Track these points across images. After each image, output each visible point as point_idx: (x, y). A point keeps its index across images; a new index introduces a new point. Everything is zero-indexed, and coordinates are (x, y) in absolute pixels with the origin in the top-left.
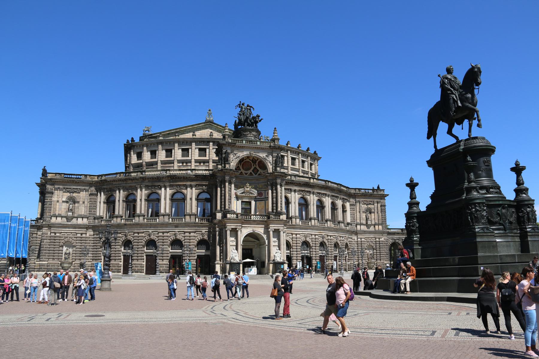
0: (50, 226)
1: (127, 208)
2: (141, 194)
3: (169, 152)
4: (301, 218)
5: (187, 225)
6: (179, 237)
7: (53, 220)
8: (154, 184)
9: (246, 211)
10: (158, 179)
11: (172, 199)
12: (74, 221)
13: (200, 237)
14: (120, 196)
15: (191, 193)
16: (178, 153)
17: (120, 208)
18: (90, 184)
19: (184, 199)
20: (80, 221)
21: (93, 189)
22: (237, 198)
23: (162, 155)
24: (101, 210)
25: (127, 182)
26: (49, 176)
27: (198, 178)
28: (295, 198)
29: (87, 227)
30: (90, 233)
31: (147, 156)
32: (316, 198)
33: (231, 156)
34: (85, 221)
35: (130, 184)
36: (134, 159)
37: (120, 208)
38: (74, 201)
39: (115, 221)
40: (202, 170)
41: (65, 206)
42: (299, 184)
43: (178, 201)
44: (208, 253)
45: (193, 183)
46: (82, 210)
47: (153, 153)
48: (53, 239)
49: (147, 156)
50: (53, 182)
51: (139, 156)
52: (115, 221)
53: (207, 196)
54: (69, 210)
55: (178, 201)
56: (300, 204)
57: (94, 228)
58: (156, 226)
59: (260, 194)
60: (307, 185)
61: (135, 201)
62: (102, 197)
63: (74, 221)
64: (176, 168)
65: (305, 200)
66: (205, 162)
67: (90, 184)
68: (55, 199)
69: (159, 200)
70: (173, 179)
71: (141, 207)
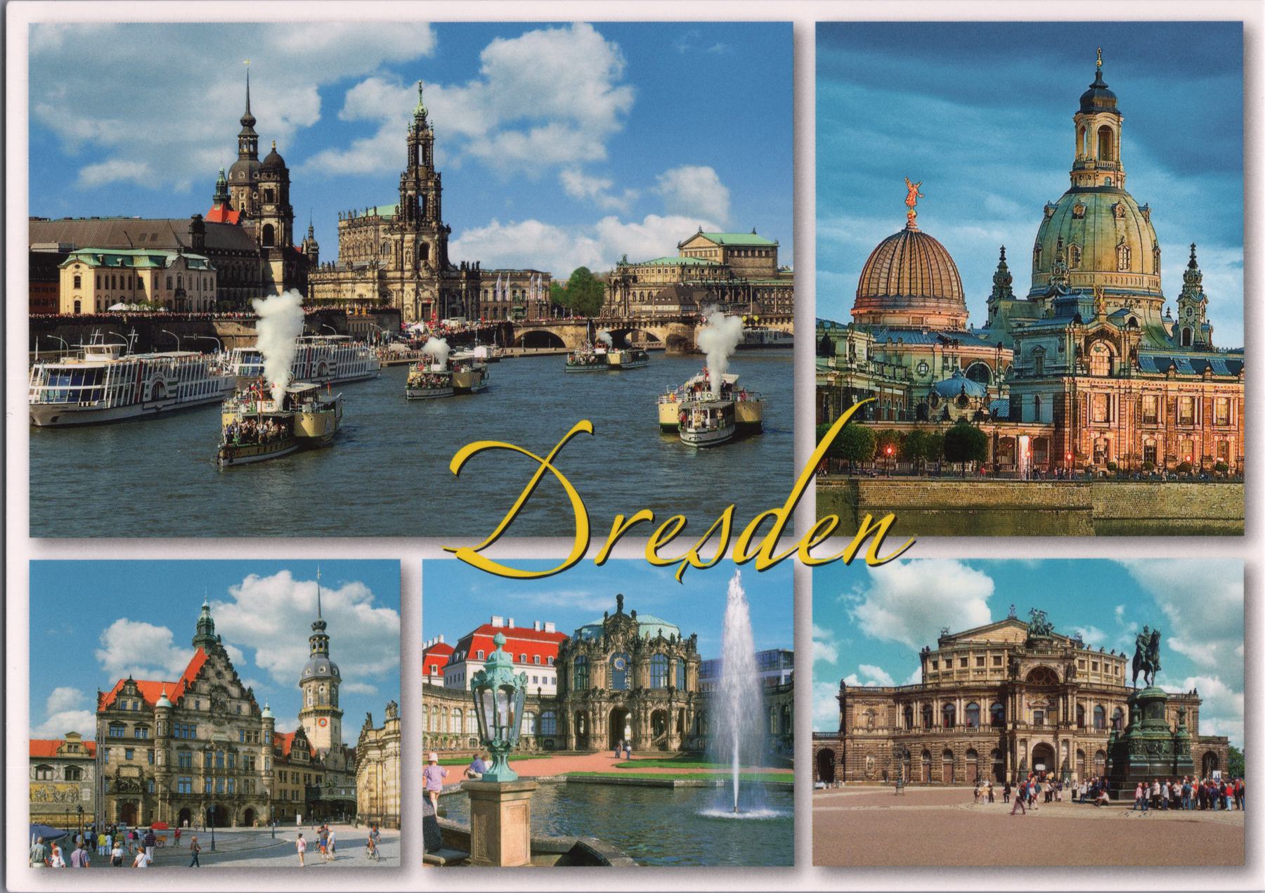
0: (852, 738)
1: (925, 718)
2: (937, 706)
3: (964, 662)
4: (1097, 727)
5: (980, 735)
6: (975, 747)
7: (855, 732)
8: (949, 695)
9: (1038, 721)
10: (953, 690)
11: (968, 711)
12: (875, 733)
13: (993, 747)
14: (917, 707)
15: (985, 705)
16: (973, 662)
17: (918, 719)
18: (888, 696)
19: (978, 710)
20: (880, 732)
21: (891, 701)
22: (1030, 707)
23: (957, 664)
24: (900, 721)
25: (922, 694)
26: (848, 690)
27: (991, 689)
28: (1090, 706)
29: (888, 738)
30: (891, 743)
31: (943, 666)
32: (1114, 706)
33: (1022, 668)
34: (886, 732)
35: (926, 696)
36: (931, 670)
37: (918, 719)
38: (874, 713)
39: (913, 732)
40: (996, 679)
41: (865, 719)
42: (1094, 693)
43: (973, 712)
44: (1001, 762)
45: (987, 694)
46: (881, 721)
47: (949, 663)
48: (856, 751)
49: (943, 666)
50: (852, 695)
51: (936, 665)
52: (913, 732)
53: (1001, 707)
54: (869, 722)
55: (973, 712)
56: (1095, 713)
57: (894, 738)
58: (952, 736)
59: (1052, 704)
60: (1104, 693)
61: (931, 712)
62: (900, 709)
63: (875, 733)
64: (971, 678)
65: (1102, 708)
66: (999, 670)
67: (888, 696)
68: (855, 711)
69: (954, 711)
70: (967, 689)
71: (938, 718)
